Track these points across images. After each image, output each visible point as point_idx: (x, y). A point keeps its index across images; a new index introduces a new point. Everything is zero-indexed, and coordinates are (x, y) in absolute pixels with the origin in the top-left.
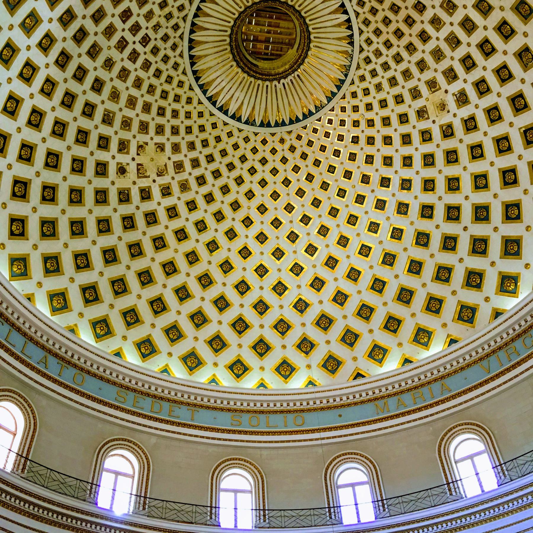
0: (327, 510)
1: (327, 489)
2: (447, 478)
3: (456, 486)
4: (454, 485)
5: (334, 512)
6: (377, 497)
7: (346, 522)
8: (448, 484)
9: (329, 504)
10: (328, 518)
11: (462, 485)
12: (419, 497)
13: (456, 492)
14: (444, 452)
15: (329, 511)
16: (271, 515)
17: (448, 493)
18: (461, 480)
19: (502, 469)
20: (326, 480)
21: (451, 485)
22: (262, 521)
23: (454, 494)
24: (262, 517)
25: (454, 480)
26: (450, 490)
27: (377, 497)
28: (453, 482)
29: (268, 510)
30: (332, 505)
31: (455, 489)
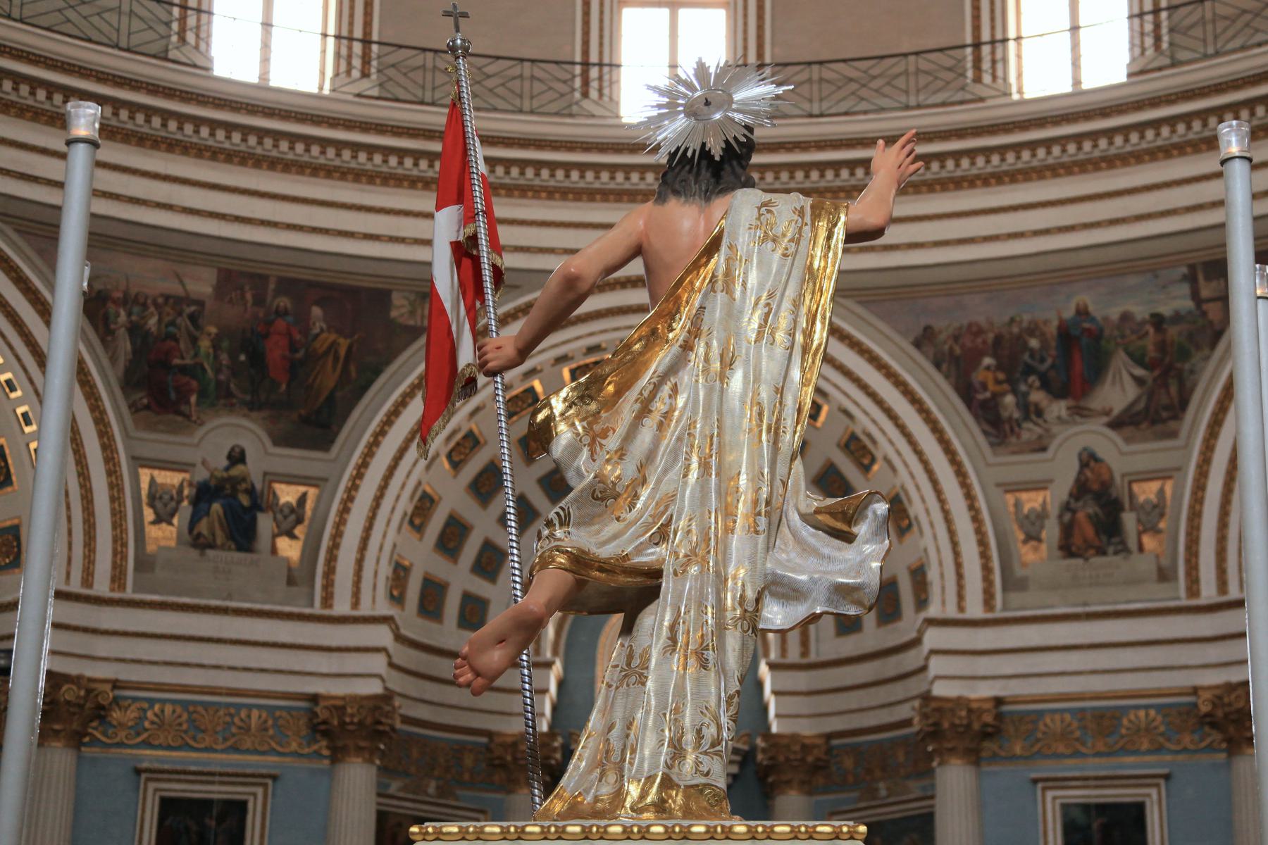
0: (578, 69)
2: (977, 28)
3: (999, 55)
4: (993, 53)
5: (600, 78)
8: (977, 45)
9: (586, 52)
10: (577, 95)
11: (1019, 57)
12: (874, 72)
17: (970, 74)
18: (1018, 38)
19: (1157, 26)
21: (986, 50)
22: (356, 73)
23: (987, 78)
24: (357, 62)
25: (999, 36)
28: (993, 42)
29: (379, 43)
30: (594, 58)
31: (994, 62)
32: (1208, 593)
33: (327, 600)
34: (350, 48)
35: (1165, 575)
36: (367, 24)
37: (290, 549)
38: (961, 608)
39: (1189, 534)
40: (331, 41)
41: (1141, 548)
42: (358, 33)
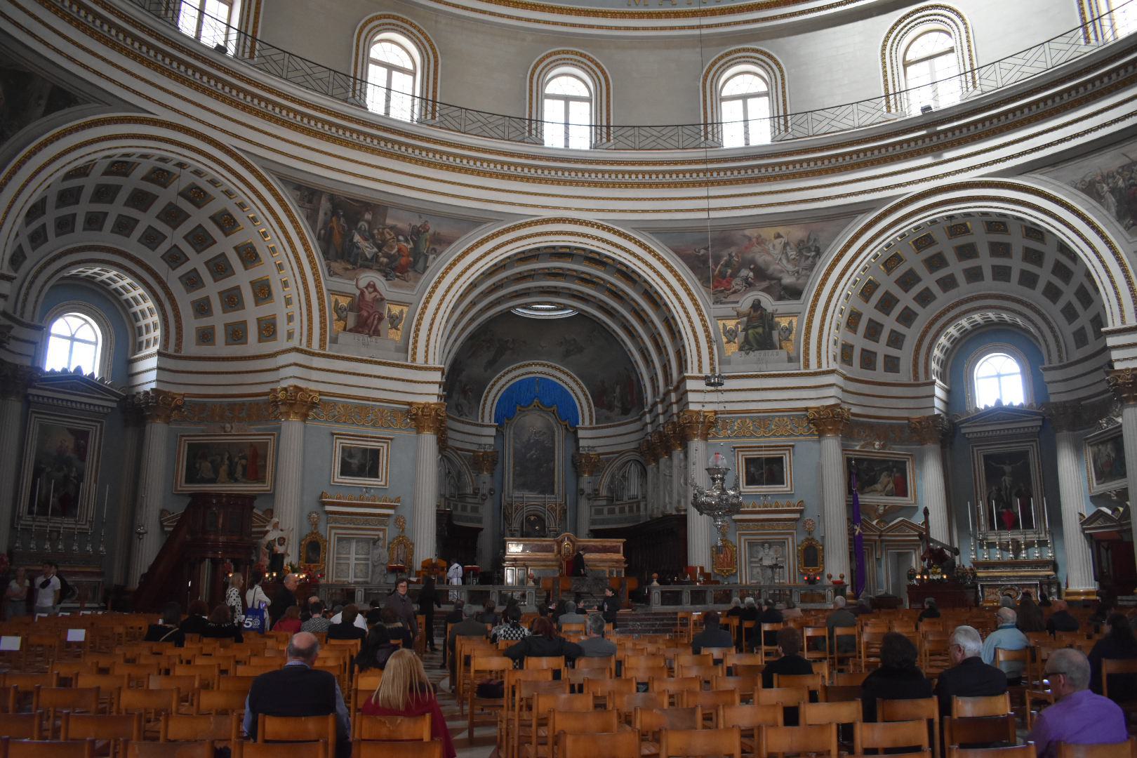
1: (531, 95)
2: (706, 117)
6: (601, 120)
7: (548, 143)
8: (706, 124)
13: (713, 136)
14: (712, 82)
15: (530, 125)
16: (445, 112)
20: (531, 82)
26: (706, 133)
27: (601, 120)
28: (713, 124)
32: (813, 367)
33: (414, 360)
34: (427, 104)
35: (790, 360)
36: (434, 96)
37: (396, 336)
38: (700, 370)
39: (805, 340)
40: (417, 101)
41: (781, 348)
42: (430, 98)
